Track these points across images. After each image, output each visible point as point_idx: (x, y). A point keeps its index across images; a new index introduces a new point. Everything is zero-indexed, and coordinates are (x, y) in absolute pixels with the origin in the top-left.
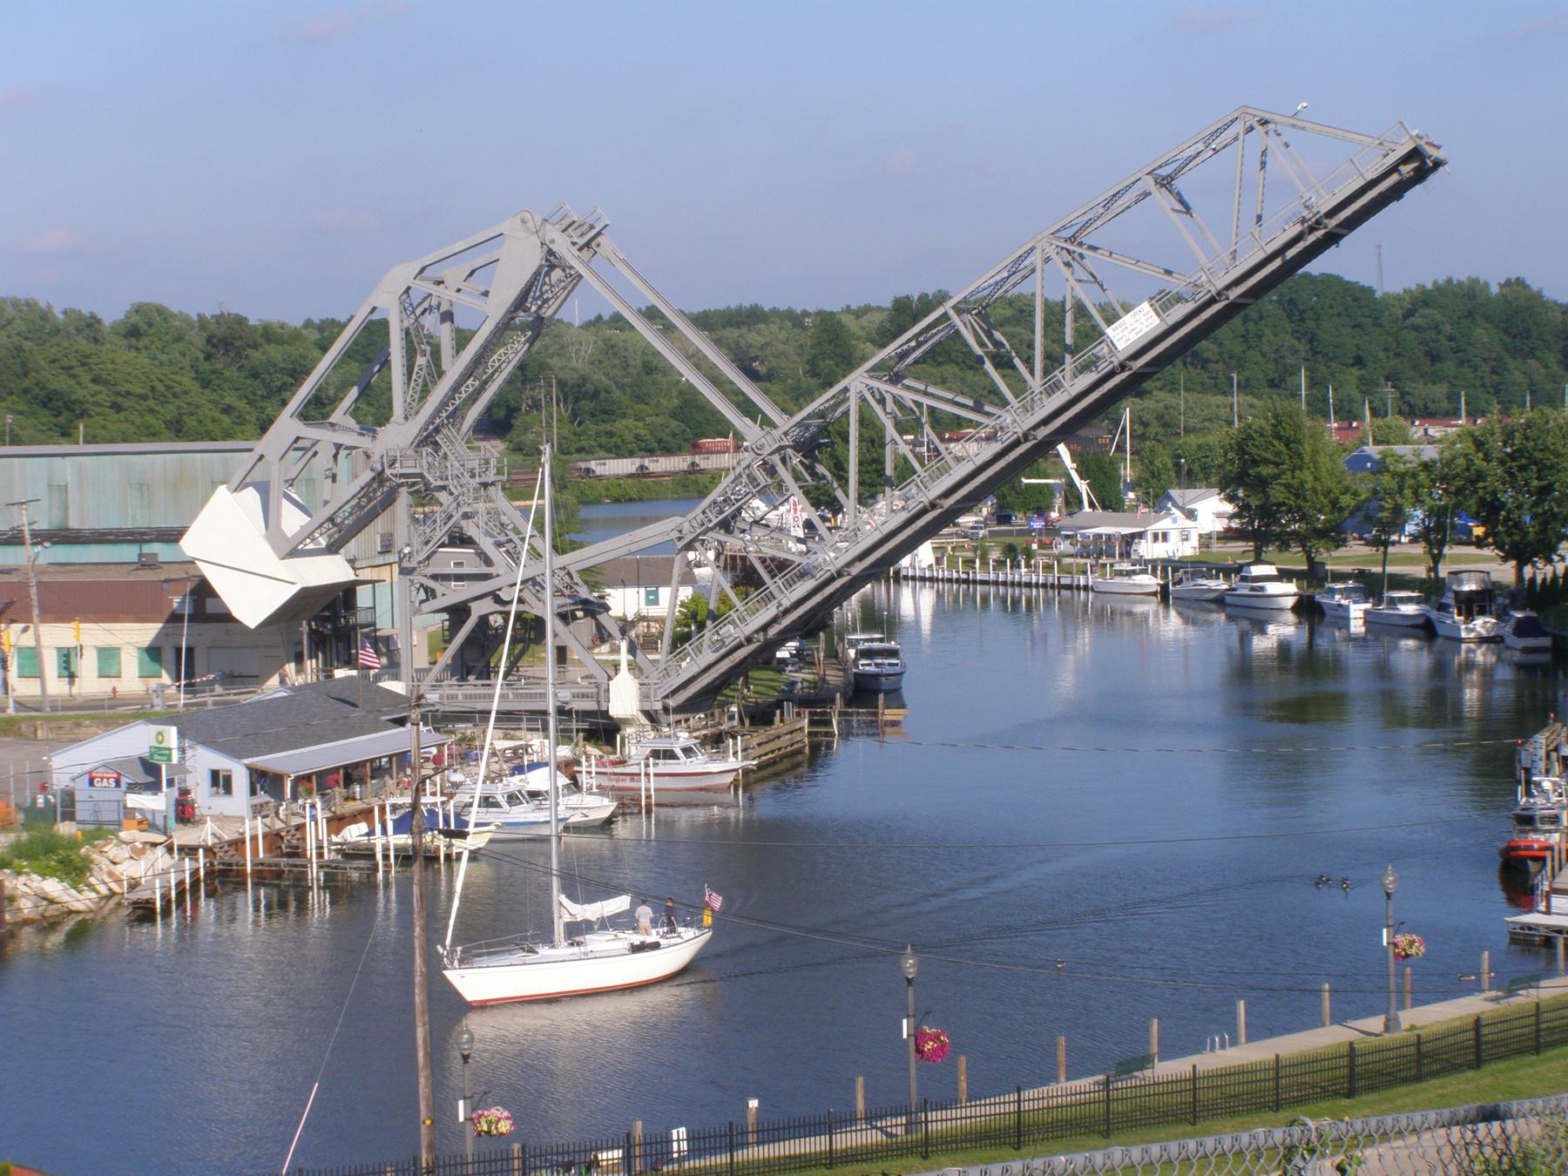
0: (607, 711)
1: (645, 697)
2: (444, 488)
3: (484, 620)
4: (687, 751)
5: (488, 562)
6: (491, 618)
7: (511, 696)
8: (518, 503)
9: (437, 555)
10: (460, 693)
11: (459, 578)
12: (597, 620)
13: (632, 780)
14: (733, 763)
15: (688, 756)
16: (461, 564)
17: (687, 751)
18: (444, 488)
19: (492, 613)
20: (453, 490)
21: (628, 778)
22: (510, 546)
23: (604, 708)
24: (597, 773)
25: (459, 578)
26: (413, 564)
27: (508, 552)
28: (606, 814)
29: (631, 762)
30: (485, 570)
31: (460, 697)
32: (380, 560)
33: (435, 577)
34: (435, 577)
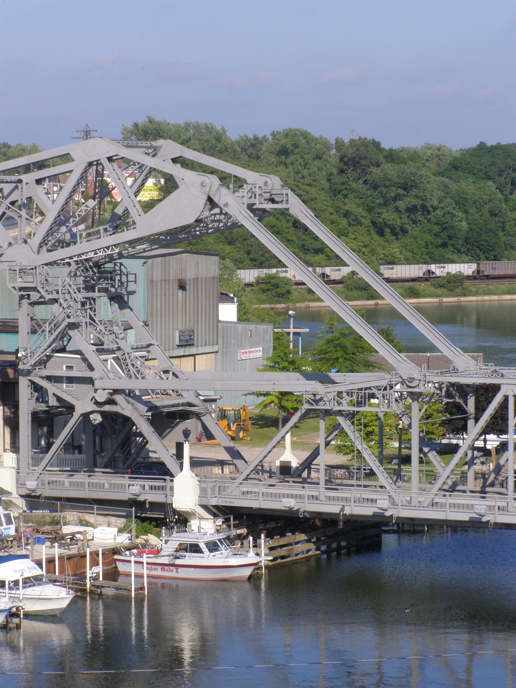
0: (172, 504)
1: (203, 491)
2: (56, 301)
3: (86, 416)
4: (213, 547)
5: (91, 368)
6: (92, 417)
7: (107, 486)
8: (351, 303)
9: (53, 359)
10: (66, 481)
11: (71, 380)
12: (201, 420)
13: (163, 569)
14: (251, 558)
15: (211, 551)
16: (70, 368)
17: (213, 547)
18: (56, 301)
19: (92, 412)
20: (62, 302)
21: (159, 567)
22: (119, 354)
23: (169, 502)
24: (136, 562)
25: (71, 380)
26: (27, 367)
27: (117, 359)
28: (63, 604)
29: (162, 553)
30: (88, 374)
31: (67, 484)
32: (181, 352)
33: (49, 378)
34: (49, 378)
